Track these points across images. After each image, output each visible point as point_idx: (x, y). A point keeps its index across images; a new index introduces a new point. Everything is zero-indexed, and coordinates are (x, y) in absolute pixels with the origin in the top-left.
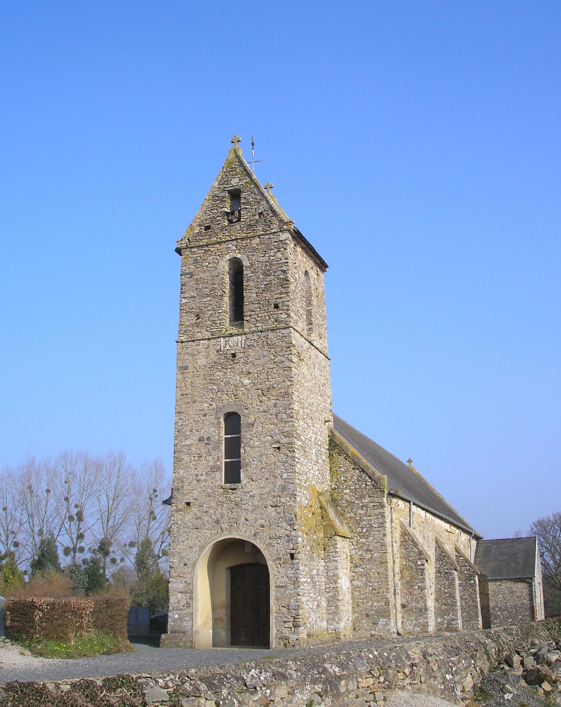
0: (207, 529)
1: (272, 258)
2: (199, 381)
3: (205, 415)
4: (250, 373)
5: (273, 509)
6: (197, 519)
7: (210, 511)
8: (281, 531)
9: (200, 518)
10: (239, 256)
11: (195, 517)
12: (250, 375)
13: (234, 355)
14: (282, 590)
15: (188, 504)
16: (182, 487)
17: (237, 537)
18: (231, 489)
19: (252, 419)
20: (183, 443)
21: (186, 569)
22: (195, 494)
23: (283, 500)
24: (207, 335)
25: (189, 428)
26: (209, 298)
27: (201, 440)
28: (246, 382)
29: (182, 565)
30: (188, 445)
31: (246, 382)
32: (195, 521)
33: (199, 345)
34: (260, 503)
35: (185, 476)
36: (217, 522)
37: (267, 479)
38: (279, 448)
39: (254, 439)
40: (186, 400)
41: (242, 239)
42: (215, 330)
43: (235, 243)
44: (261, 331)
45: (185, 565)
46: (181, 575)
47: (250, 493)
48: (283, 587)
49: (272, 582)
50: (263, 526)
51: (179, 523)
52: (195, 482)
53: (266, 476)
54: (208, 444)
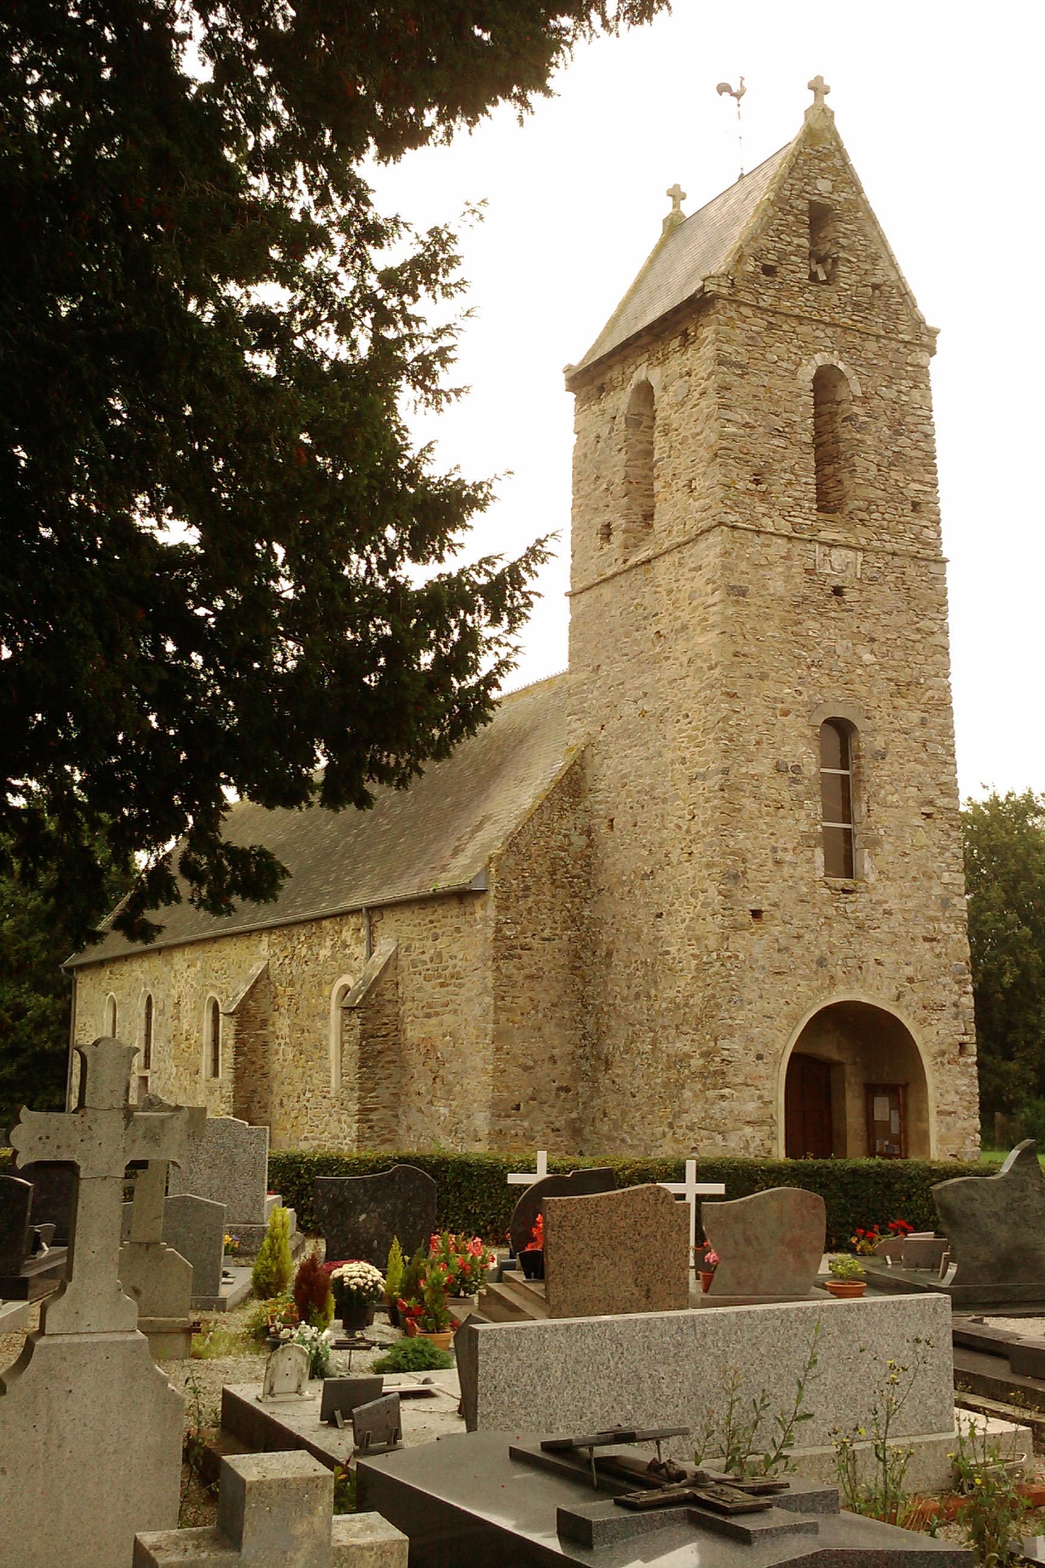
0: (804, 977)
1: (904, 398)
2: (771, 630)
3: (786, 714)
4: (873, 640)
5: (927, 945)
6: (779, 950)
7: (807, 937)
8: (944, 994)
9: (787, 949)
10: (841, 366)
11: (776, 946)
12: (875, 646)
13: (838, 591)
14: (948, 1119)
15: (756, 914)
16: (744, 873)
17: (865, 1000)
18: (844, 891)
19: (879, 743)
20: (743, 770)
21: (762, 1069)
22: (774, 892)
23: (943, 927)
24: (786, 528)
25: (753, 738)
26: (781, 442)
27: (780, 768)
28: (868, 658)
29: (751, 1058)
30: (753, 776)
31: (868, 658)
32: (776, 955)
33: (768, 546)
34: (903, 929)
35: (750, 847)
36: (821, 962)
37: (914, 879)
38: (929, 816)
39: (887, 787)
40: (746, 669)
41: (846, 329)
42: (801, 521)
43: (829, 331)
44: (894, 554)
45: (759, 1057)
46: (750, 1082)
47: (886, 906)
48: (950, 1113)
49: (932, 1104)
50: (910, 980)
51: (741, 956)
52: (770, 864)
53: (913, 874)
54: (795, 781)
